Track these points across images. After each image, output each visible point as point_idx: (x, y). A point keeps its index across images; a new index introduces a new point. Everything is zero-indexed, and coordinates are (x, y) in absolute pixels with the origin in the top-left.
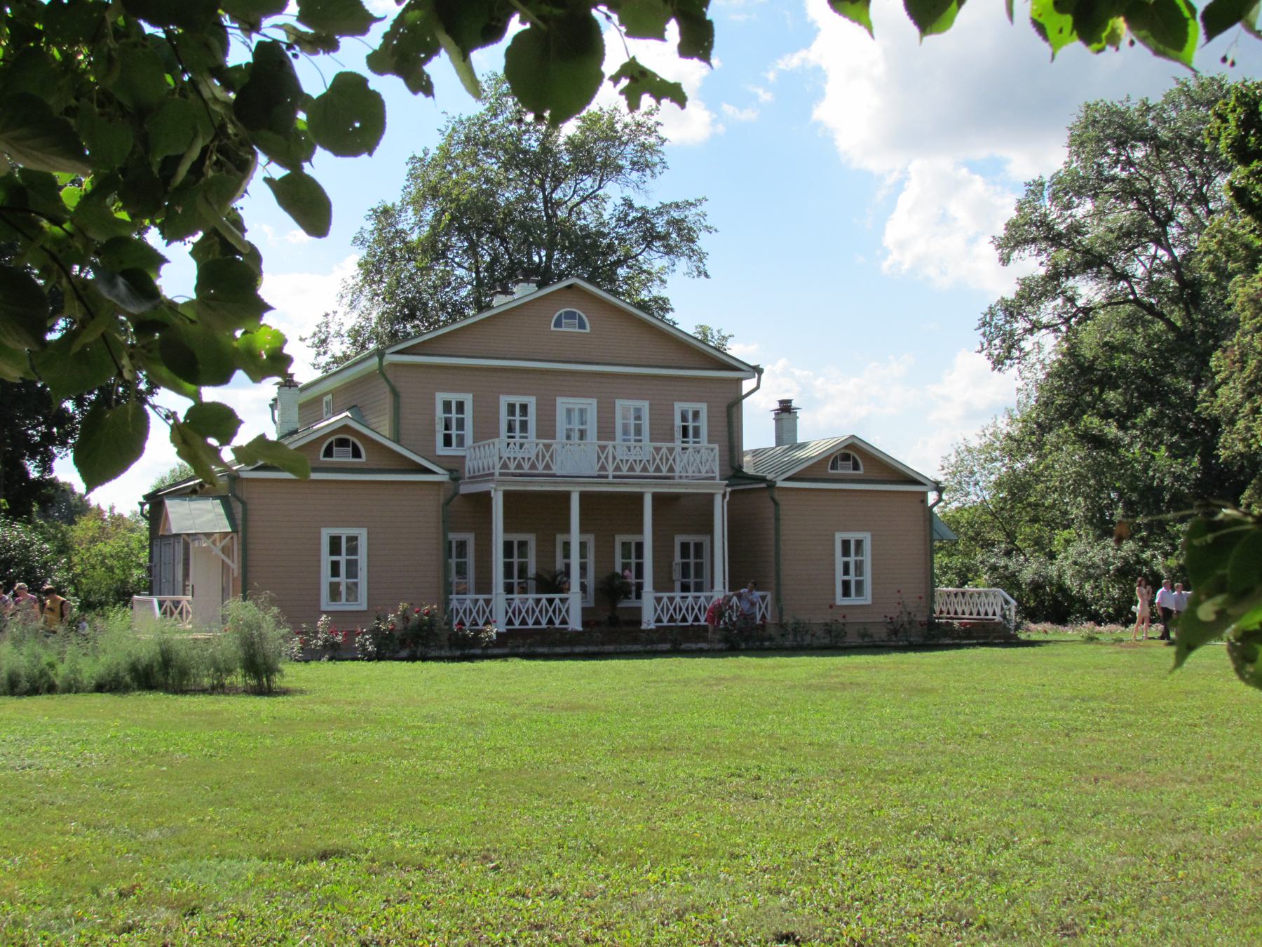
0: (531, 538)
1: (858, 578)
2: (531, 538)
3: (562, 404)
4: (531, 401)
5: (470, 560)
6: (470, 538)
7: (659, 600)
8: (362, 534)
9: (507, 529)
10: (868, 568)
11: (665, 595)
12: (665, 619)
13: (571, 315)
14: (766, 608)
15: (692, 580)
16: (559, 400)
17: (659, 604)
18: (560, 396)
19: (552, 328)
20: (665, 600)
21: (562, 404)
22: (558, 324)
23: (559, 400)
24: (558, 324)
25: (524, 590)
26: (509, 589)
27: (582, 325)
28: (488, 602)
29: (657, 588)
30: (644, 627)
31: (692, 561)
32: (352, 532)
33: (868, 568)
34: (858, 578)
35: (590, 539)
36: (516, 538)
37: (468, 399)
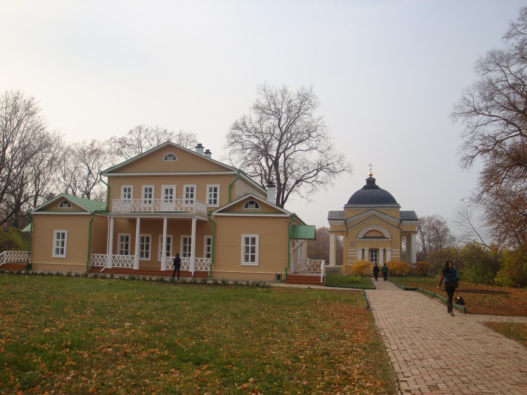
0: (150, 236)
1: (248, 254)
2: (150, 236)
3: (164, 188)
4: (153, 187)
5: (129, 243)
6: (130, 235)
7: (197, 260)
8: (257, 237)
9: (141, 232)
10: (55, 243)
11: (199, 259)
12: (199, 268)
13: (170, 155)
14: (93, 260)
15: (187, 252)
16: (163, 186)
17: (197, 262)
18: (143, 184)
19: (164, 160)
20: (199, 261)
21: (164, 188)
22: (166, 159)
23: (163, 186)
24: (166, 159)
25: (126, 253)
26: (115, 252)
27: (174, 159)
28: (133, 258)
29: (196, 256)
30: (162, 270)
31: (145, 243)
32: (253, 236)
33: (55, 243)
34: (248, 254)
35: (171, 237)
36: (145, 236)
37: (132, 187)
